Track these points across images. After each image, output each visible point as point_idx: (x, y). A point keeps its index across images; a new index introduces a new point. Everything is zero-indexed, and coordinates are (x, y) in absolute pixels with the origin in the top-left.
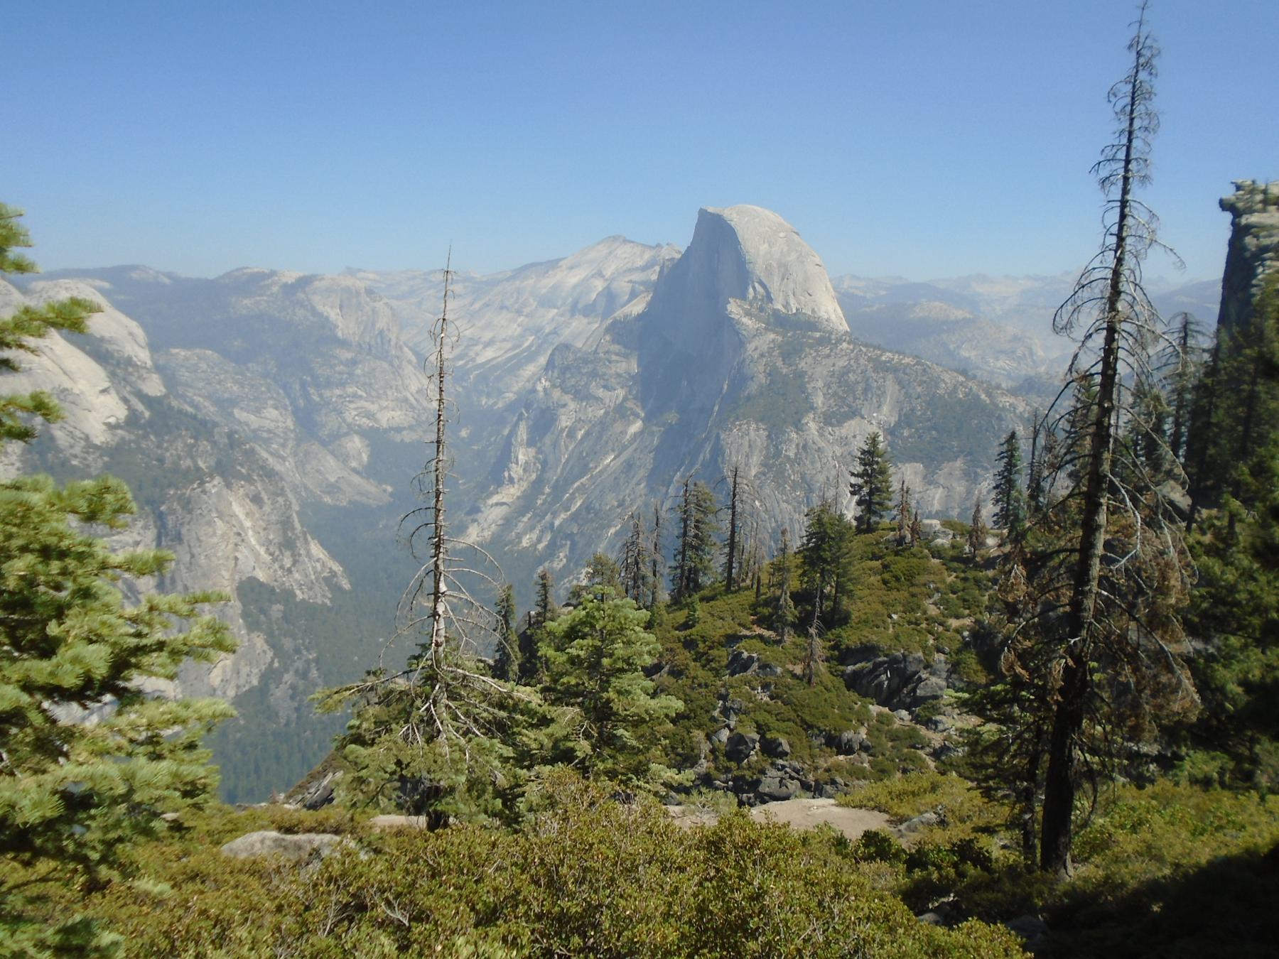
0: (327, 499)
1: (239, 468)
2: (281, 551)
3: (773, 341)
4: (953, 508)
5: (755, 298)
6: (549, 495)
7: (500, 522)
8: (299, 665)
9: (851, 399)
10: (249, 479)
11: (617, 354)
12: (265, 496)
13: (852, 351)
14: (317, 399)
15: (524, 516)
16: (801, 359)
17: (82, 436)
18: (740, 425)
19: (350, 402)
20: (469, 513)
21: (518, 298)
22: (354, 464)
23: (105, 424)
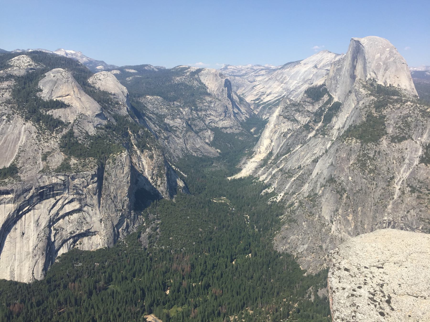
0: (194, 154)
1: (147, 145)
2: (157, 178)
3: (373, 100)
5: (370, 79)
6: (273, 160)
7: (254, 169)
8: (153, 225)
9: (407, 130)
10: (150, 150)
11: (308, 102)
12: (155, 156)
13: (412, 106)
16: (384, 109)
17: (85, 132)
18: (348, 140)
19: (208, 117)
20: (244, 164)
21: (282, 76)
22: (207, 141)
23: (96, 127)
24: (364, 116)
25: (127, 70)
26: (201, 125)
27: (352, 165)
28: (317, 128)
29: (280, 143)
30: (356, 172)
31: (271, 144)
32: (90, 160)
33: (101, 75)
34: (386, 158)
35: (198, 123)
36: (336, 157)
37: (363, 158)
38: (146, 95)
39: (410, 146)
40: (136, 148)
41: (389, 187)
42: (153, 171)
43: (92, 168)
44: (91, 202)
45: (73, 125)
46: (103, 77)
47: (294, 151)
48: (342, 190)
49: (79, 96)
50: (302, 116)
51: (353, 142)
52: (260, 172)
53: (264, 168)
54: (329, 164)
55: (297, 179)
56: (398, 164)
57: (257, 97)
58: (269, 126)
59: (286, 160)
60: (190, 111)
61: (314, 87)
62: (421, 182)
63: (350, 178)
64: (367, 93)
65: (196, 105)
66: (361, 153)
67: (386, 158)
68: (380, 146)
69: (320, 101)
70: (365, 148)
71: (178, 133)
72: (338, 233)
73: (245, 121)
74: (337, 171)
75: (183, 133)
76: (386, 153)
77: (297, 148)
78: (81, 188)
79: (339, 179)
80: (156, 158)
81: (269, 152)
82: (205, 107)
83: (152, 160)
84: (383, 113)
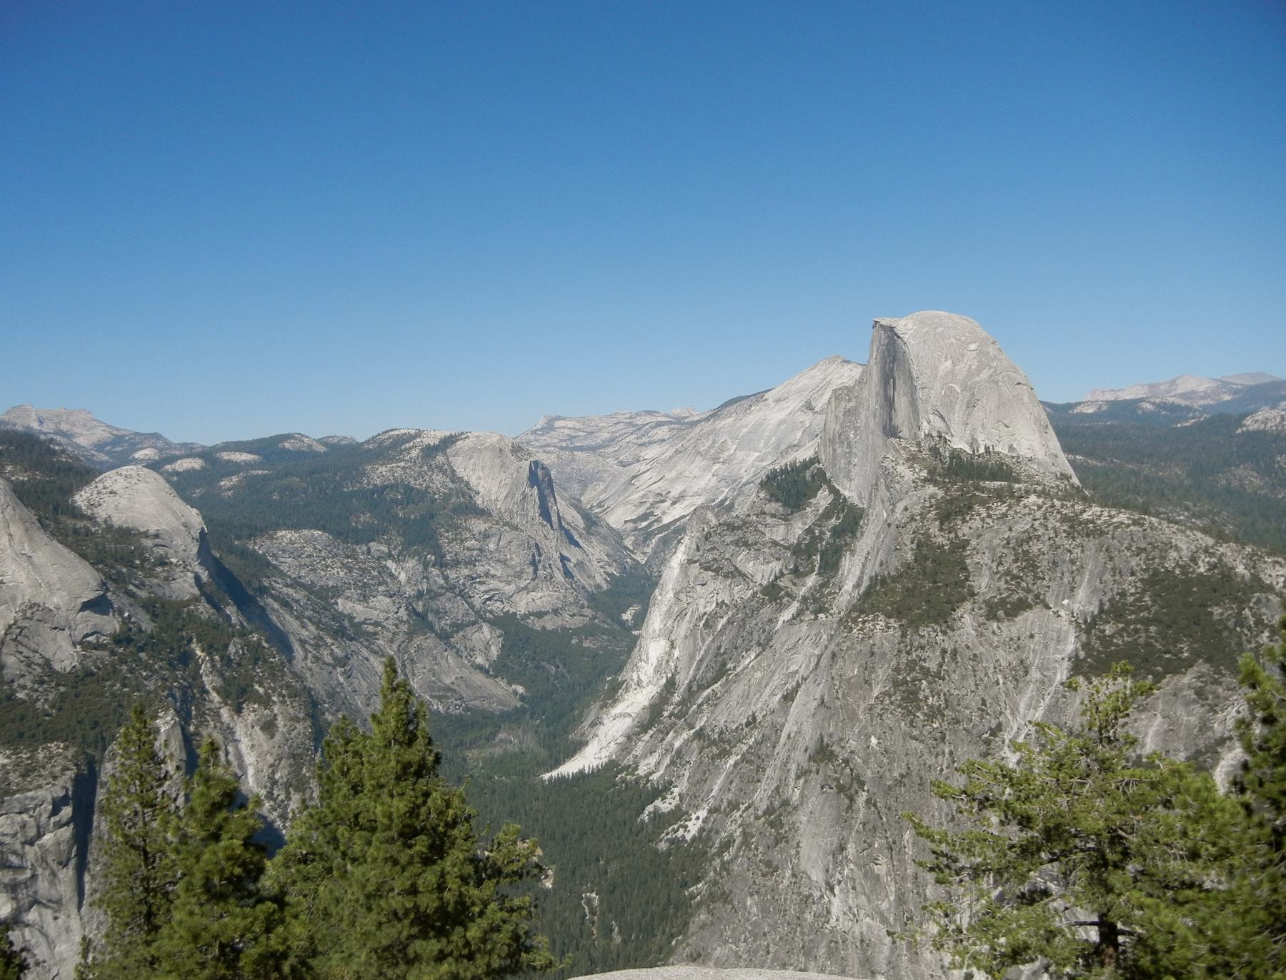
0: (438, 706)
1: (257, 687)
3: (931, 497)
5: (929, 435)
6: (679, 704)
7: (621, 740)
10: (266, 702)
11: (773, 516)
12: (280, 722)
15: (646, 732)
16: (964, 521)
17: (41, 661)
19: (480, 583)
20: (593, 725)
21: (714, 442)
22: (480, 660)
23: (81, 643)
24: (910, 546)
25: (226, 456)
26: (457, 609)
27: (877, 698)
28: (803, 591)
29: (696, 649)
30: (889, 720)
31: (669, 654)
32: (51, 752)
33: (117, 478)
34: (974, 671)
35: (448, 605)
36: (833, 678)
37: (908, 675)
38: (275, 530)
39: (1041, 627)
40: (215, 696)
41: (989, 757)
42: (273, 773)
43: (55, 778)
44: (53, 892)
46: (125, 484)
47: (738, 670)
48: (852, 780)
49: (27, 550)
50: (757, 558)
51: (878, 627)
52: (639, 748)
53: (651, 732)
54: (815, 704)
55: (742, 761)
56: (1011, 686)
57: (642, 510)
58: (660, 598)
59: (714, 701)
60: (421, 568)
61: (786, 468)
63: (874, 741)
64: (916, 476)
65: (439, 547)
66: (904, 660)
67: (974, 671)
70: (912, 645)
71: (381, 642)
72: (850, 923)
73: (605, 587)
74: (837, 724)
75: (399, 642)
76: (975, 655)
77: (747, 662)
78: (18, 847)
79: (843, 748)
80: (285, 730)
81: (664, 681)
82: (468, 553)
83: (272, 737)
84: (960, 534)
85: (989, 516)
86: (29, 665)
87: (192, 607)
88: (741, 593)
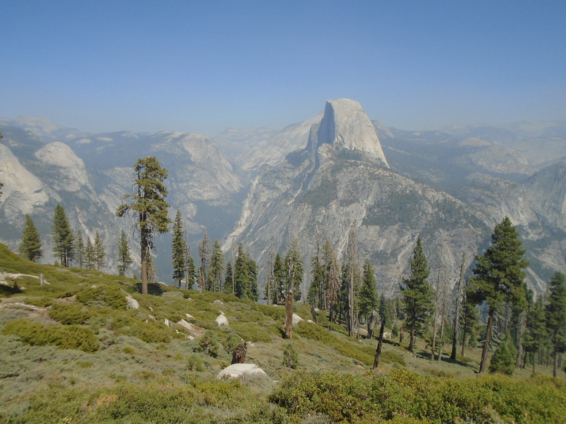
1: (99, 222)
2: (108, 259)
3: (331, 164)
4: (389, 249)
6: (252, 232)
9: (355, 193)
10: (102, 228)
11: (289, 168)
12: (107, 235)
13: (363, 169)
14: (176, 187)
16: (339, 173)
19: (190, 189)
22: (189, 216)
23: (33, 205)
25: (100, 139)
31: (251, 215)
45: (4, 205)
46: (55, 149)
57: (255, 164)
62: (361, 244)
68: (330, 210)
69: (301, 167)
82: (186, 178)
84: (336, 177)
85: (347, 172)
86: (13, 212)
87: (77, 194)
88: (276, 194)
